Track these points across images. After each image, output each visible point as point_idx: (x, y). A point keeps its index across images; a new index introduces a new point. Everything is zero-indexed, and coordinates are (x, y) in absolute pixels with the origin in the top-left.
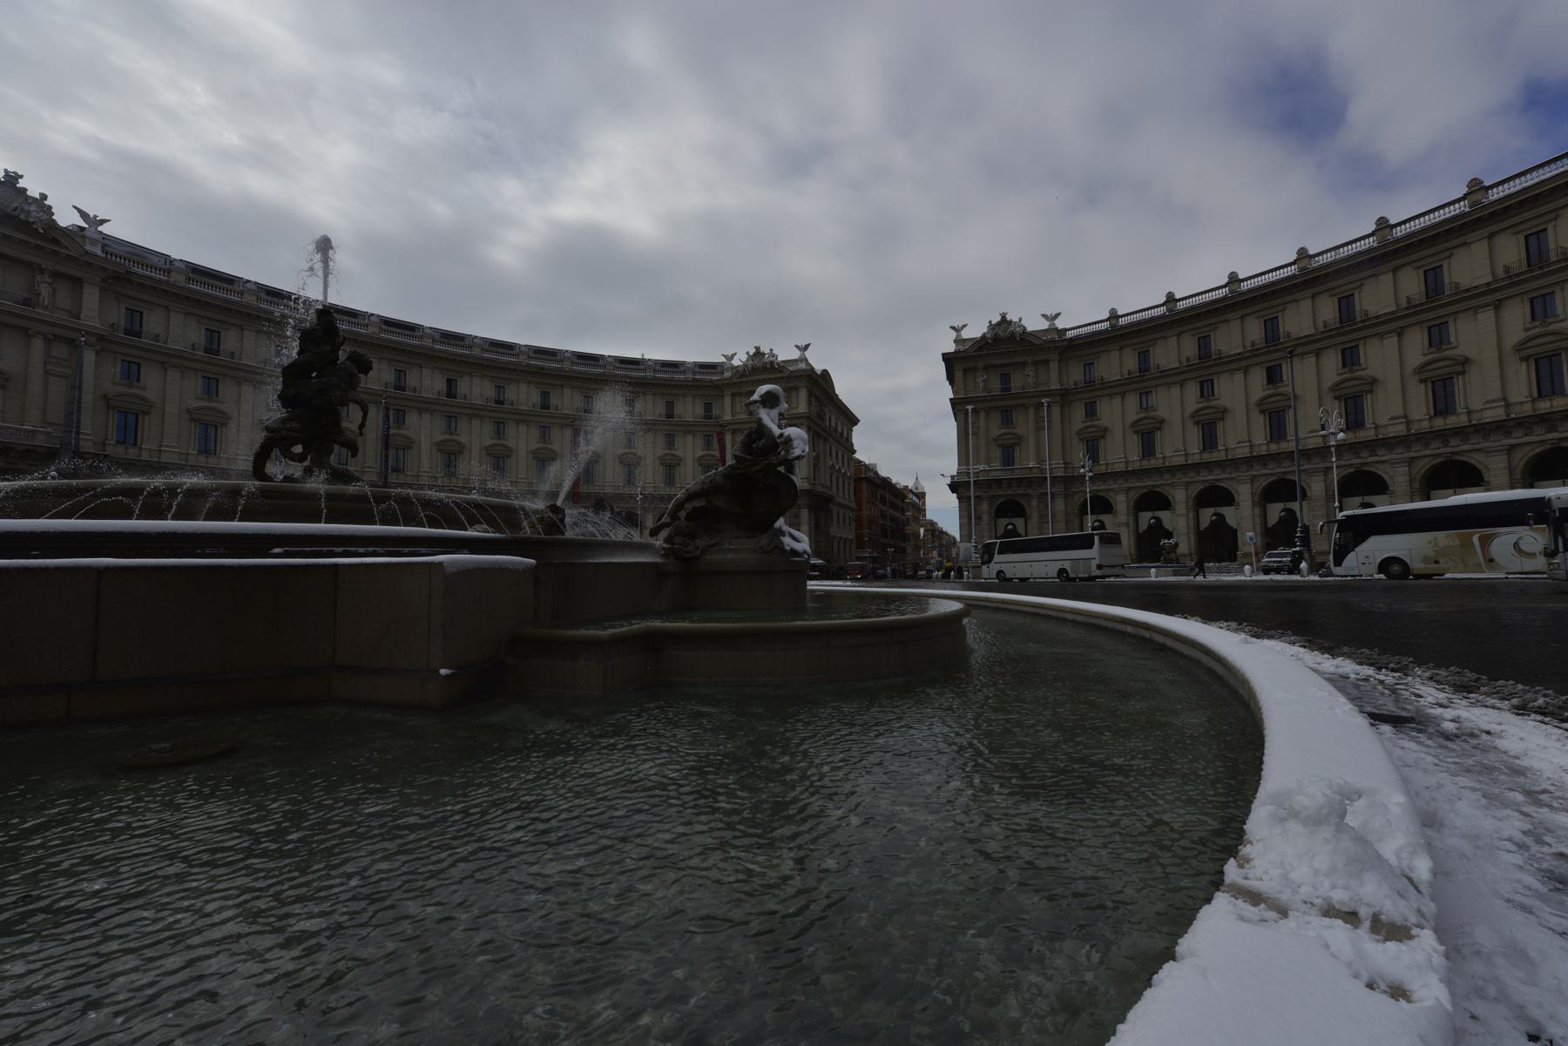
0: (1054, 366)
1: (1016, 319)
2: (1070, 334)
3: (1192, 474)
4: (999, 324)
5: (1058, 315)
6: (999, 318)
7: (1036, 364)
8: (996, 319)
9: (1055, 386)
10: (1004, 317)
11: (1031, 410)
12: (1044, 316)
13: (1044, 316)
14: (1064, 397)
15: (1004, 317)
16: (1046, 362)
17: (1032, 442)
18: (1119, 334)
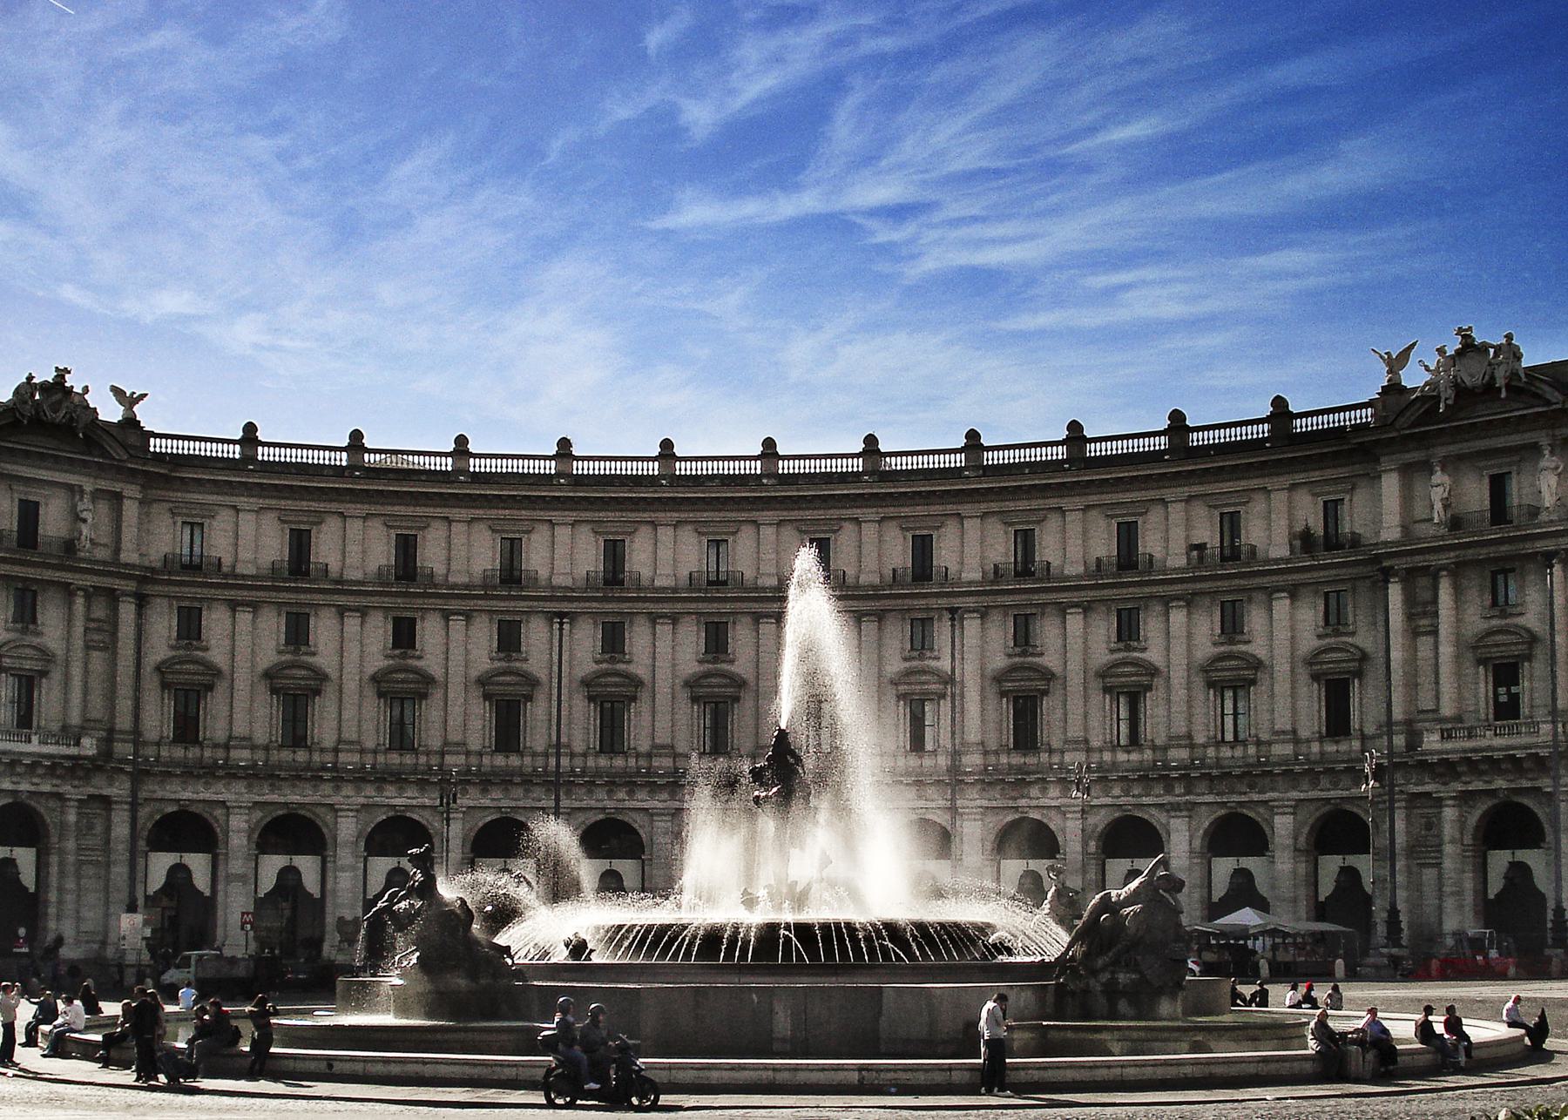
0: (131, 510)
1: (77, 389)
2: (155, 445)
3: (370, 790)
4: (45, 387)
5: (144, 396)
6: (50, 377)
7: (97, 495)
8: (45, 375)
9: (129, 556)
10: (61, 374)
11: (80, 602)
12: (118, 392)
13: (118, 392)
14: (146, 583)
15: (61, 374)
16: (117, 498)
17: (76, 672)
18: (248, 471)
